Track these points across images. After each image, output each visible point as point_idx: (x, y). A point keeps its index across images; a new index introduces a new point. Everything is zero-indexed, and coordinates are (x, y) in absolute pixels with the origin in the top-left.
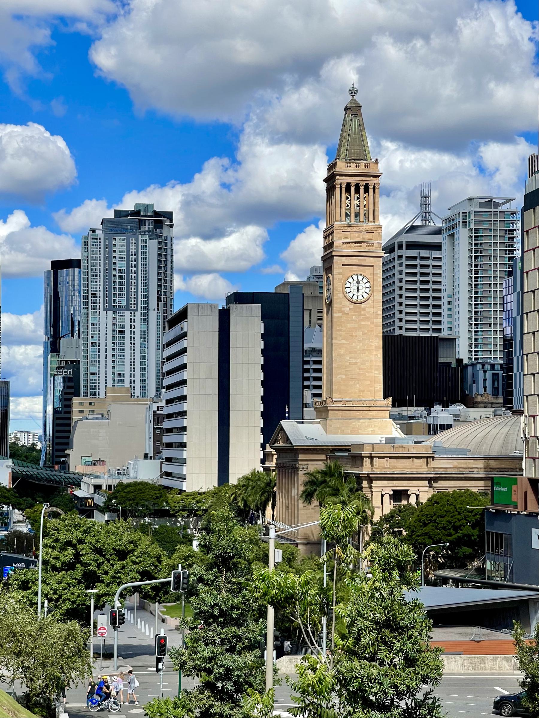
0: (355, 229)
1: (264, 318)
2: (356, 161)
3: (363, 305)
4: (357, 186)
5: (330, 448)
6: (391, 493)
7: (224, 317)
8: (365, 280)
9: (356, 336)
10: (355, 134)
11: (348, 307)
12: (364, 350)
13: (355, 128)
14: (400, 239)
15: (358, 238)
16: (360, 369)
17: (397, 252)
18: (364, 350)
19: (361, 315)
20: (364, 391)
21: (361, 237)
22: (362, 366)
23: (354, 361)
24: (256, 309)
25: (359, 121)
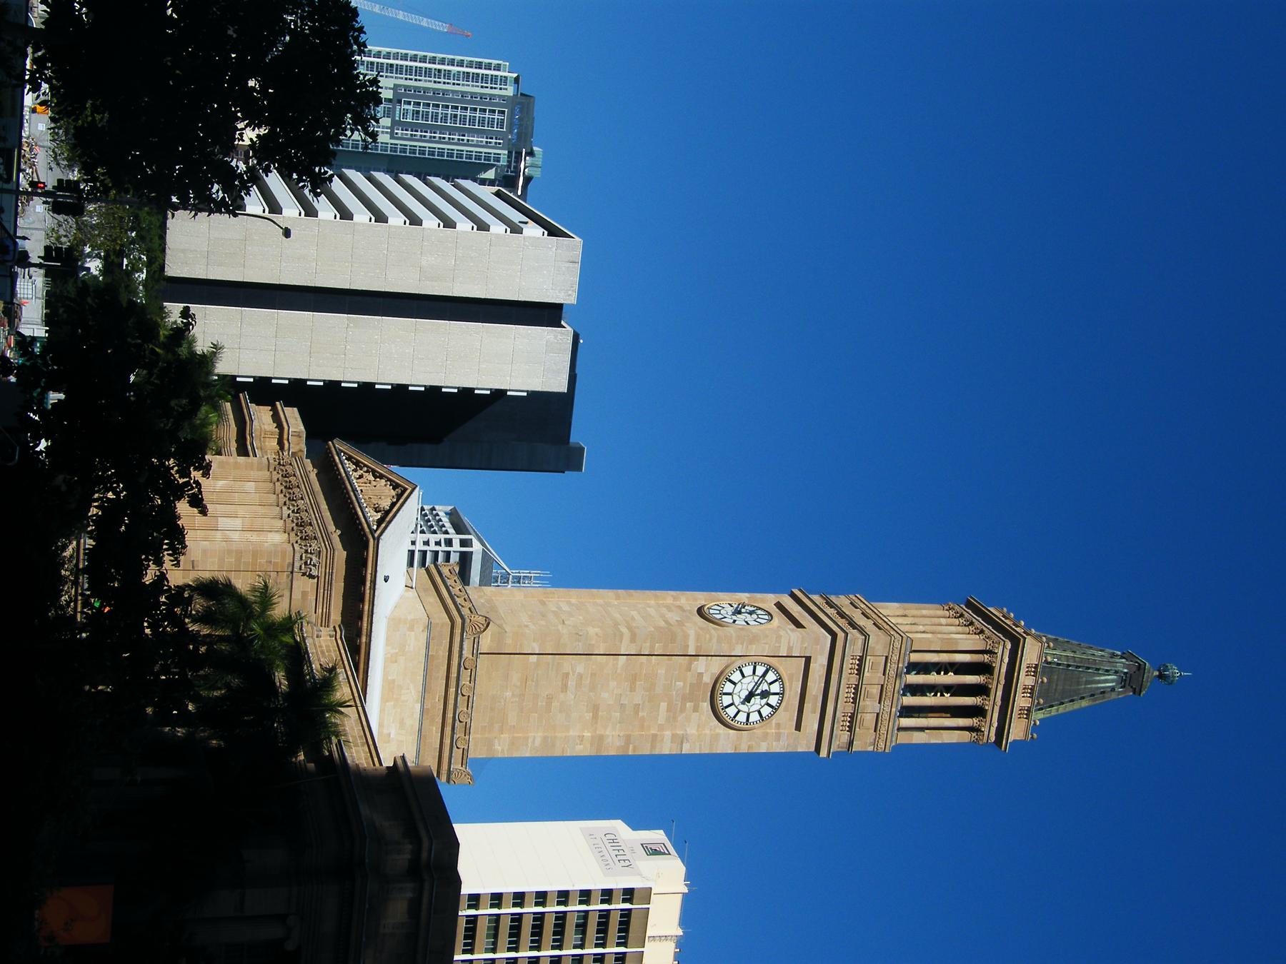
0: (890, 688)
1: (536, 398)
3: (706, 706)
4: (981, 690)
5: (364, 639)
7: (546, 314)
8: (766, 711)
9: (632, 689)
10: (1088, 682)
11: (707, 669)
12: (595, 709)
13: (1099, 682)
14: (476, 543)
16: (550, 699)
17: (456, 539)
18: (595, 709)
19: (685, 699)
20: (492, 709)
21: (868, 702)
22: (555, 704)
23: (571, 683)
25: (1113, 689)
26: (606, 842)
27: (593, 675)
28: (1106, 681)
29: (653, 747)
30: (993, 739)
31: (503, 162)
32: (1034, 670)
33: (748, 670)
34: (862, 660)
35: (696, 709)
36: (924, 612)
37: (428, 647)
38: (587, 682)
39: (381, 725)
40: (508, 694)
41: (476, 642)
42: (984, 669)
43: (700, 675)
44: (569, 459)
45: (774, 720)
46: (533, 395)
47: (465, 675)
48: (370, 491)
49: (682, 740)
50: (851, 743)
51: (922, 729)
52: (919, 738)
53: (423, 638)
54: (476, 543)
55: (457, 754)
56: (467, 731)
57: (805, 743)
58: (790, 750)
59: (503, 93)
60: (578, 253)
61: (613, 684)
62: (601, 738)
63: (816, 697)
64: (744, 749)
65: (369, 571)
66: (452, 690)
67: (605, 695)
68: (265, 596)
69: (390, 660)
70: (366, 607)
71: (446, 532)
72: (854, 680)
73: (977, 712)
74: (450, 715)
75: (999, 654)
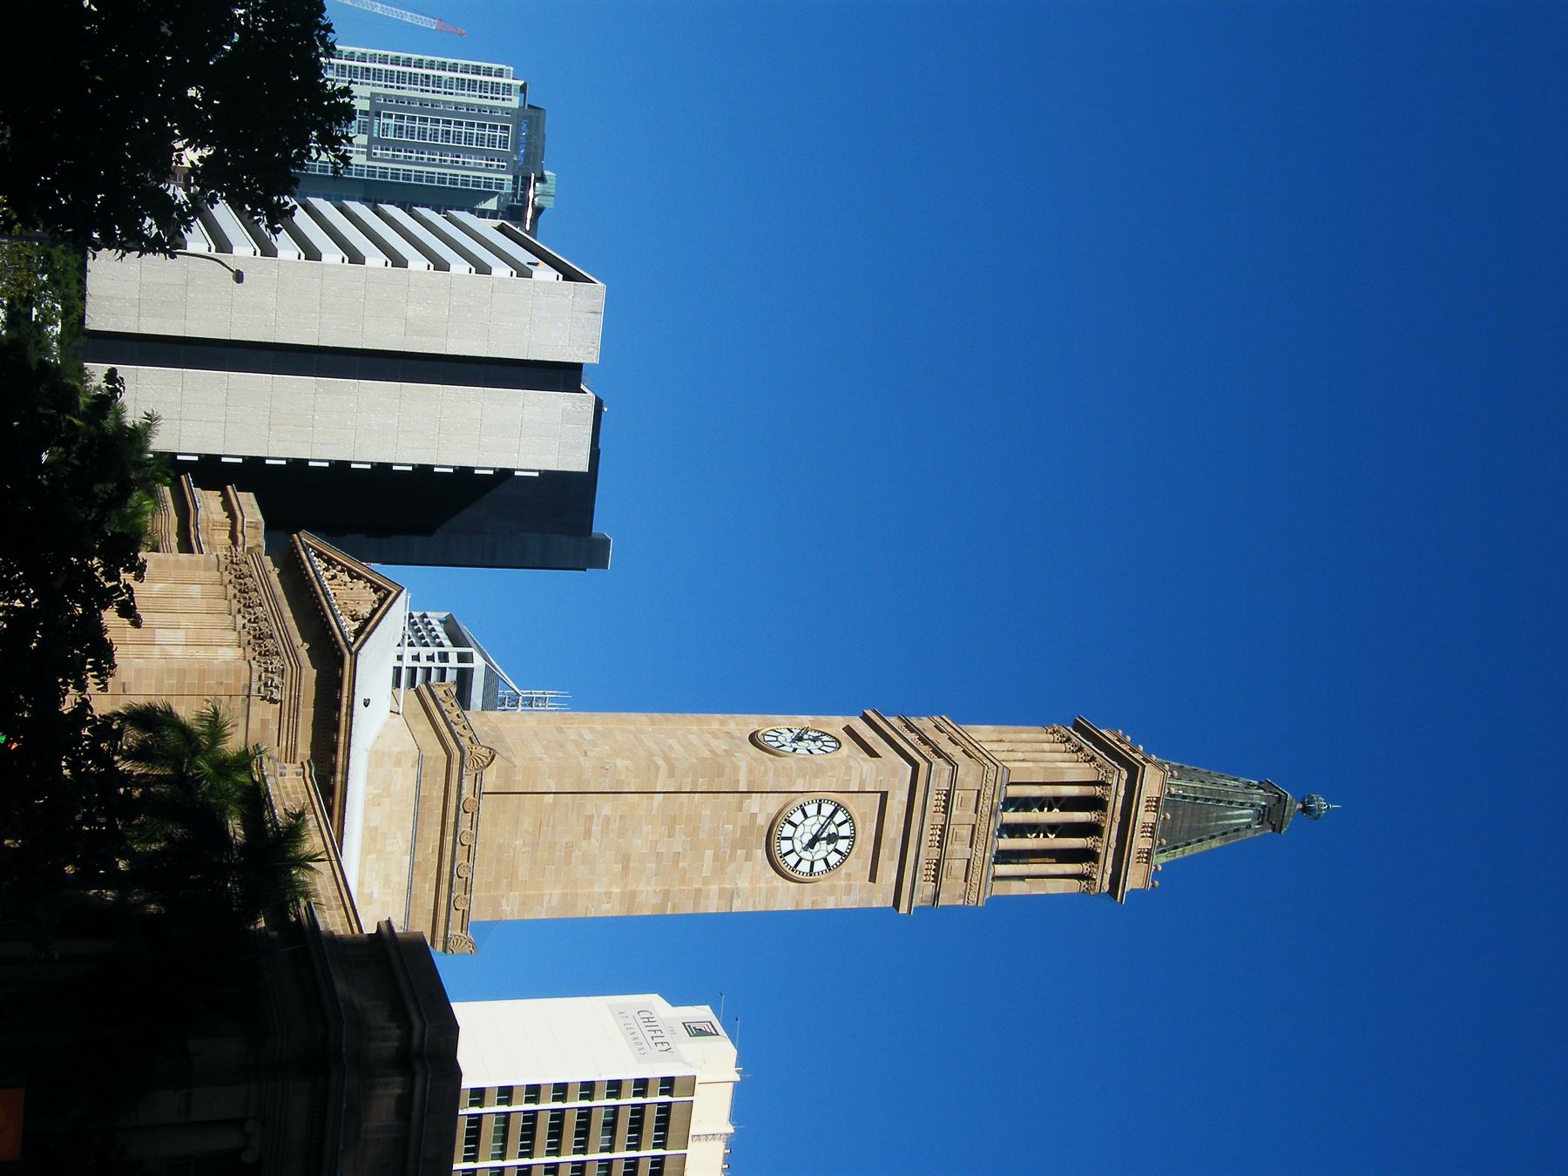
0: (983, 828)
1: (550, 479)
2: (1158, 827)
3: (761, 853)
4: (1092, 830)
5: (339, 777)
6: (248, 1158)
7: (562, 376)
8: (834, 859)
11: (762, 809)
12: (626, 859)
13: (1232, 817)
14: (477, 657)
15: (956, 837)
16: (570, 847)
17: (453, 653)
18: (626, 859)
19: (735, 845)
20: (499, 861)
22: (576, 853)
23: (596, 828)
24: (580, 464)
25: (1249, 826)
26: (640, 1021)
27: (622, 818)
28: (1241, 816)
29: (696, 903)
30: (1106, 888)
31: (508, 189)
32: (1155, 805)
33: (811, 810)
34: (948, 794)
35: (748, 858)
36: (1024, 736)
37: (418, 787)
38: (615, 826)
39: (361, 884)
40: (518, 842)
41: (478, 779)
42: (1096, 804)
43: (754, 816)
44: (592, 554)
45: (844, 869)
46: (548, 476)
47: (465, 820)
48: (346, 596)
49: (731, 895)
50: (936, 896)
51: (1021, 878)
52: (1017, 888)
53: (415, 771)
54: (477, 657)
55: (456, 916)
56: (468, 888)
57: (881, 896)
58: (863, 905)
59: (506, 104)
60: (600, 302)
61: (647, 828)
62: (633, 894)
63: (894, 840)
64: (807, 905)
65: (345, 694)
66: (449, 839)
67: (638, 842)
68: (215, 726)
69: (372, 802)
70: (342, 738)
71: (441, 645)
72: (939, 819)
73: (1088, 855)
74: (446, 869)
75: (1114, 786)
